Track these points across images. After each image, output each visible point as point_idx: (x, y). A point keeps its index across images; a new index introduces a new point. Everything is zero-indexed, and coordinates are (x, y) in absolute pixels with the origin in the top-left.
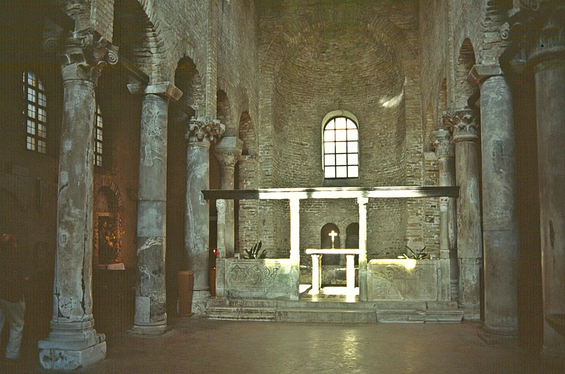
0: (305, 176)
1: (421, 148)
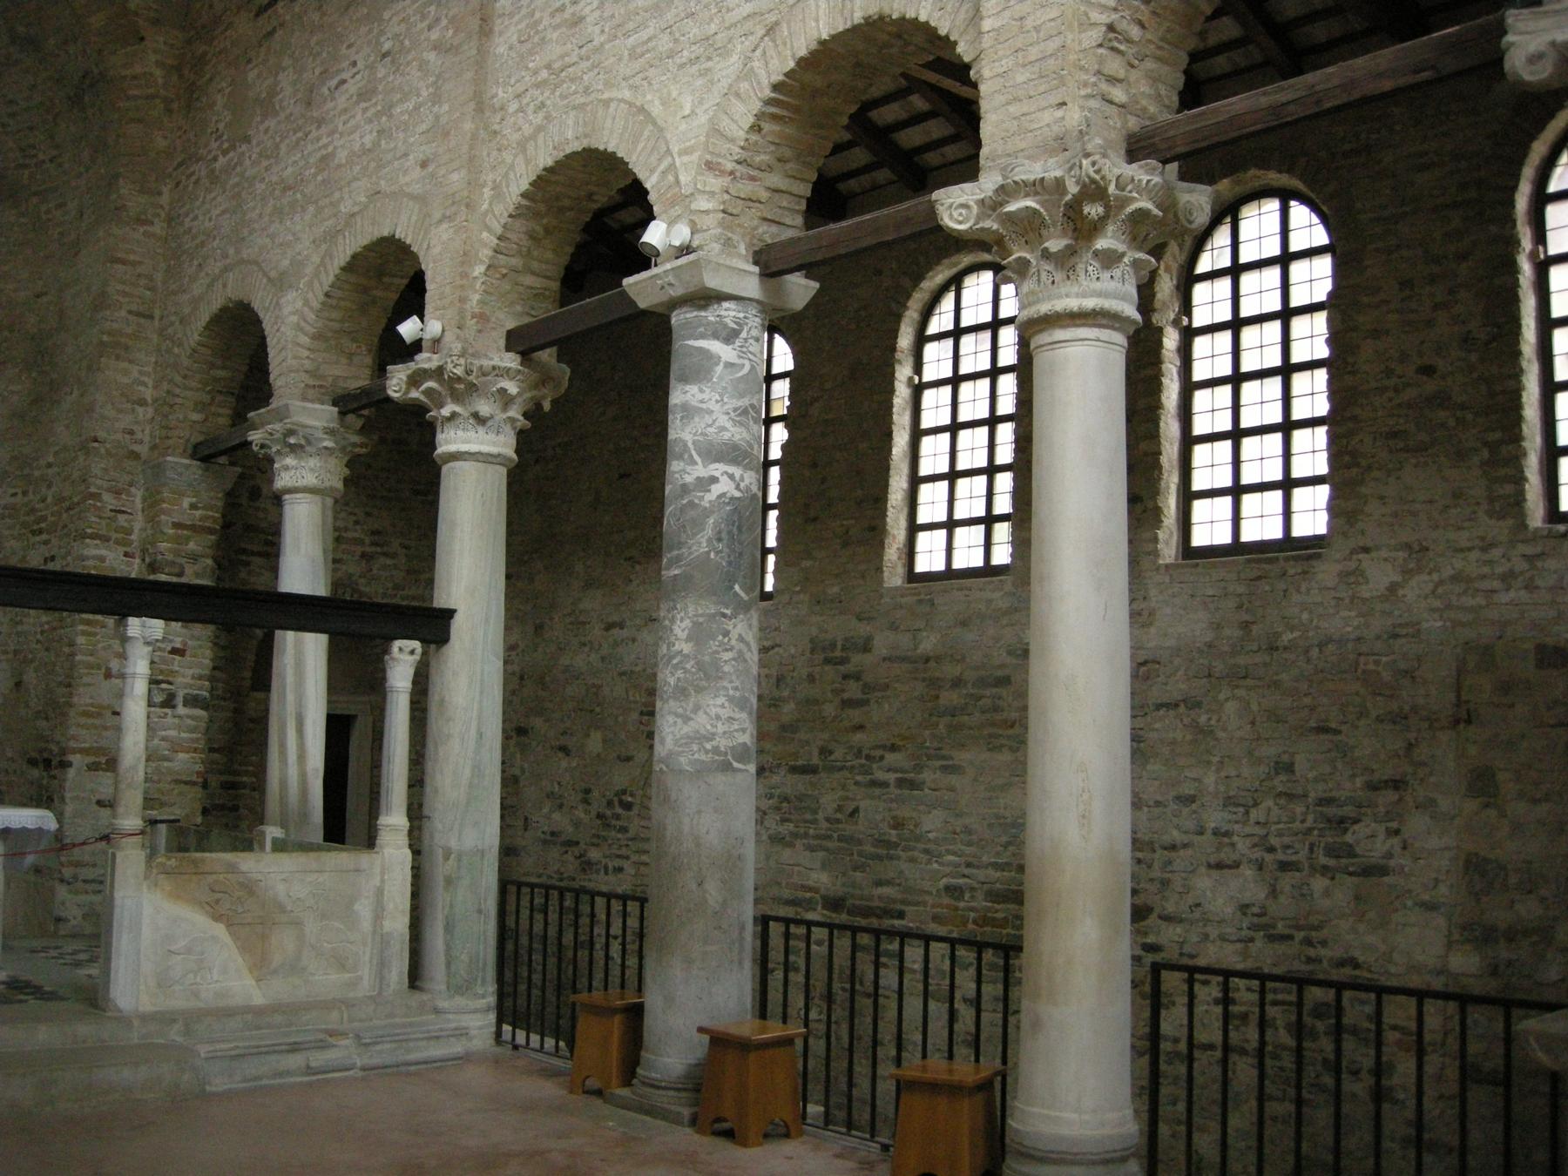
1: (141, 442)
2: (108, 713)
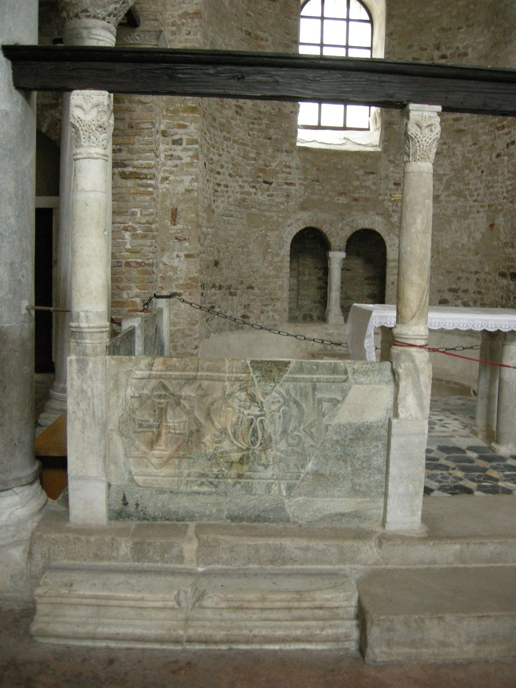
0: (260, 112)
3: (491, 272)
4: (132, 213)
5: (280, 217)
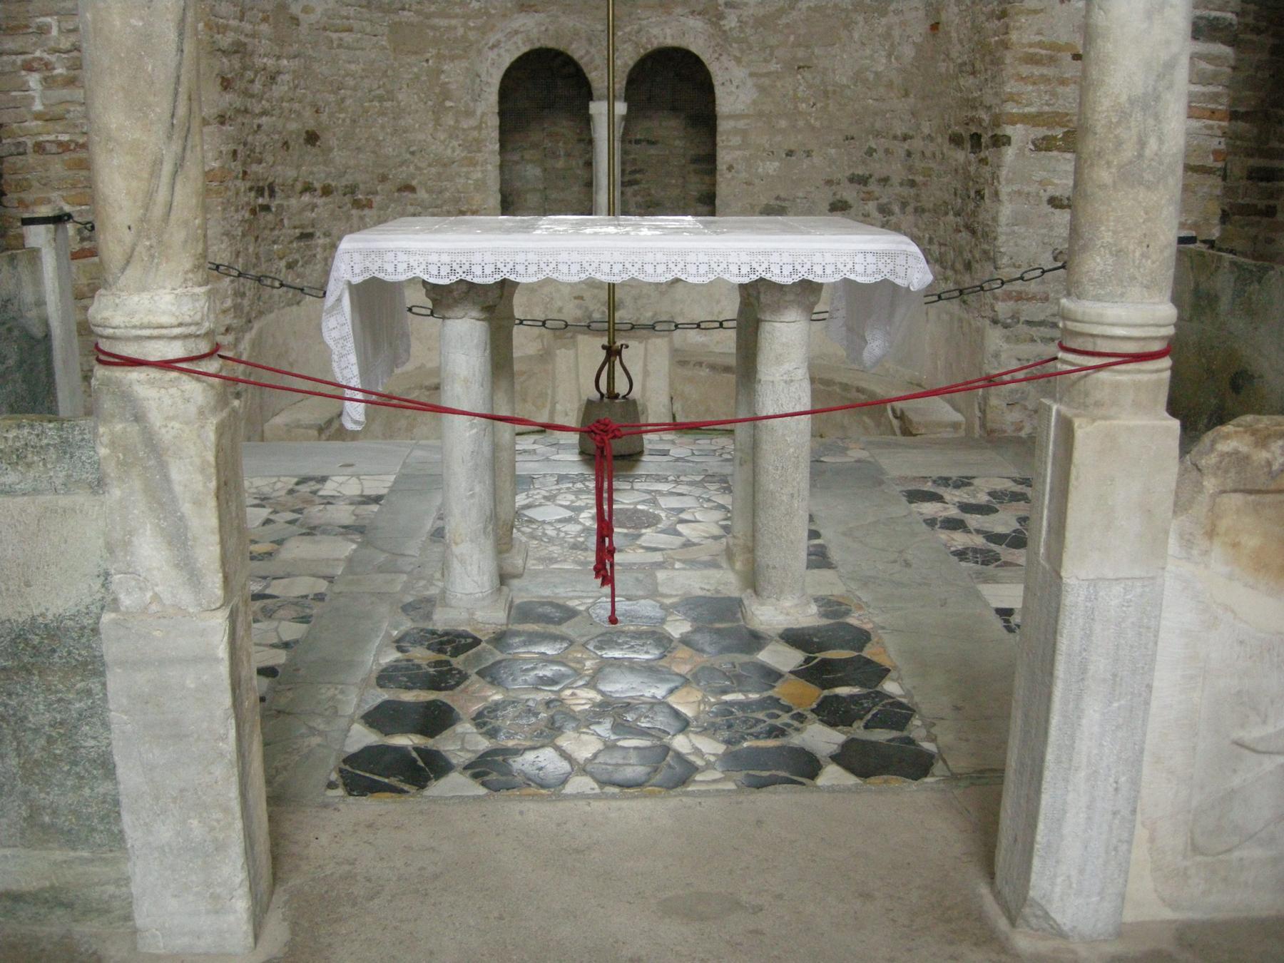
2: (1067, 57)
3: (933, 135)
4: (39, 28)
5: (470, 29)
